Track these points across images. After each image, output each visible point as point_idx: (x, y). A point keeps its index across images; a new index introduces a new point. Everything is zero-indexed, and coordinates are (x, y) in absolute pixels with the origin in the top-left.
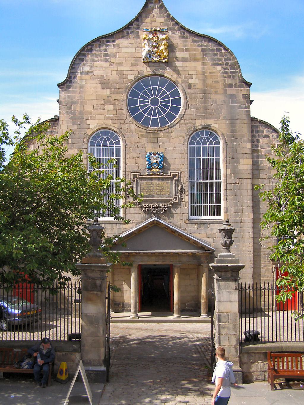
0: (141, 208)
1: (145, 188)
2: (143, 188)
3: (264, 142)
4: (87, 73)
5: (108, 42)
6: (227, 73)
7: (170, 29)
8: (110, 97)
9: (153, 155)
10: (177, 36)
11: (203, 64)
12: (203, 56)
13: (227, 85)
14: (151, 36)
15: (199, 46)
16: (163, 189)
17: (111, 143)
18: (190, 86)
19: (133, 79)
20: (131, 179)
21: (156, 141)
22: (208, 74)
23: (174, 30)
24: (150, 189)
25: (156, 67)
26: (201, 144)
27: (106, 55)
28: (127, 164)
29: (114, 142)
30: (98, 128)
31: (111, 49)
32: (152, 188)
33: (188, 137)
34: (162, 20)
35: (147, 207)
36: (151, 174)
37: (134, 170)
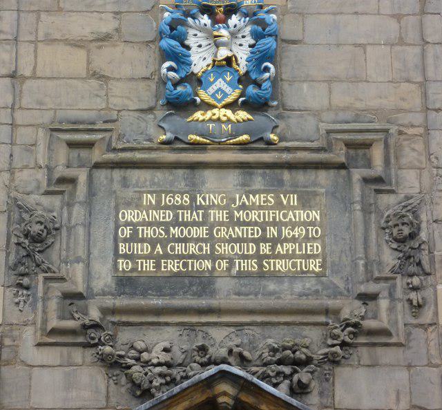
0: (113, 364)
1: (149, 232)
2: (135, 232)
9: (205, 20)
16: (274, 242)
20: (50, 169)
24: (185, 240)
32: (202, 232)
35: (164, 357)
37: (74, 114)
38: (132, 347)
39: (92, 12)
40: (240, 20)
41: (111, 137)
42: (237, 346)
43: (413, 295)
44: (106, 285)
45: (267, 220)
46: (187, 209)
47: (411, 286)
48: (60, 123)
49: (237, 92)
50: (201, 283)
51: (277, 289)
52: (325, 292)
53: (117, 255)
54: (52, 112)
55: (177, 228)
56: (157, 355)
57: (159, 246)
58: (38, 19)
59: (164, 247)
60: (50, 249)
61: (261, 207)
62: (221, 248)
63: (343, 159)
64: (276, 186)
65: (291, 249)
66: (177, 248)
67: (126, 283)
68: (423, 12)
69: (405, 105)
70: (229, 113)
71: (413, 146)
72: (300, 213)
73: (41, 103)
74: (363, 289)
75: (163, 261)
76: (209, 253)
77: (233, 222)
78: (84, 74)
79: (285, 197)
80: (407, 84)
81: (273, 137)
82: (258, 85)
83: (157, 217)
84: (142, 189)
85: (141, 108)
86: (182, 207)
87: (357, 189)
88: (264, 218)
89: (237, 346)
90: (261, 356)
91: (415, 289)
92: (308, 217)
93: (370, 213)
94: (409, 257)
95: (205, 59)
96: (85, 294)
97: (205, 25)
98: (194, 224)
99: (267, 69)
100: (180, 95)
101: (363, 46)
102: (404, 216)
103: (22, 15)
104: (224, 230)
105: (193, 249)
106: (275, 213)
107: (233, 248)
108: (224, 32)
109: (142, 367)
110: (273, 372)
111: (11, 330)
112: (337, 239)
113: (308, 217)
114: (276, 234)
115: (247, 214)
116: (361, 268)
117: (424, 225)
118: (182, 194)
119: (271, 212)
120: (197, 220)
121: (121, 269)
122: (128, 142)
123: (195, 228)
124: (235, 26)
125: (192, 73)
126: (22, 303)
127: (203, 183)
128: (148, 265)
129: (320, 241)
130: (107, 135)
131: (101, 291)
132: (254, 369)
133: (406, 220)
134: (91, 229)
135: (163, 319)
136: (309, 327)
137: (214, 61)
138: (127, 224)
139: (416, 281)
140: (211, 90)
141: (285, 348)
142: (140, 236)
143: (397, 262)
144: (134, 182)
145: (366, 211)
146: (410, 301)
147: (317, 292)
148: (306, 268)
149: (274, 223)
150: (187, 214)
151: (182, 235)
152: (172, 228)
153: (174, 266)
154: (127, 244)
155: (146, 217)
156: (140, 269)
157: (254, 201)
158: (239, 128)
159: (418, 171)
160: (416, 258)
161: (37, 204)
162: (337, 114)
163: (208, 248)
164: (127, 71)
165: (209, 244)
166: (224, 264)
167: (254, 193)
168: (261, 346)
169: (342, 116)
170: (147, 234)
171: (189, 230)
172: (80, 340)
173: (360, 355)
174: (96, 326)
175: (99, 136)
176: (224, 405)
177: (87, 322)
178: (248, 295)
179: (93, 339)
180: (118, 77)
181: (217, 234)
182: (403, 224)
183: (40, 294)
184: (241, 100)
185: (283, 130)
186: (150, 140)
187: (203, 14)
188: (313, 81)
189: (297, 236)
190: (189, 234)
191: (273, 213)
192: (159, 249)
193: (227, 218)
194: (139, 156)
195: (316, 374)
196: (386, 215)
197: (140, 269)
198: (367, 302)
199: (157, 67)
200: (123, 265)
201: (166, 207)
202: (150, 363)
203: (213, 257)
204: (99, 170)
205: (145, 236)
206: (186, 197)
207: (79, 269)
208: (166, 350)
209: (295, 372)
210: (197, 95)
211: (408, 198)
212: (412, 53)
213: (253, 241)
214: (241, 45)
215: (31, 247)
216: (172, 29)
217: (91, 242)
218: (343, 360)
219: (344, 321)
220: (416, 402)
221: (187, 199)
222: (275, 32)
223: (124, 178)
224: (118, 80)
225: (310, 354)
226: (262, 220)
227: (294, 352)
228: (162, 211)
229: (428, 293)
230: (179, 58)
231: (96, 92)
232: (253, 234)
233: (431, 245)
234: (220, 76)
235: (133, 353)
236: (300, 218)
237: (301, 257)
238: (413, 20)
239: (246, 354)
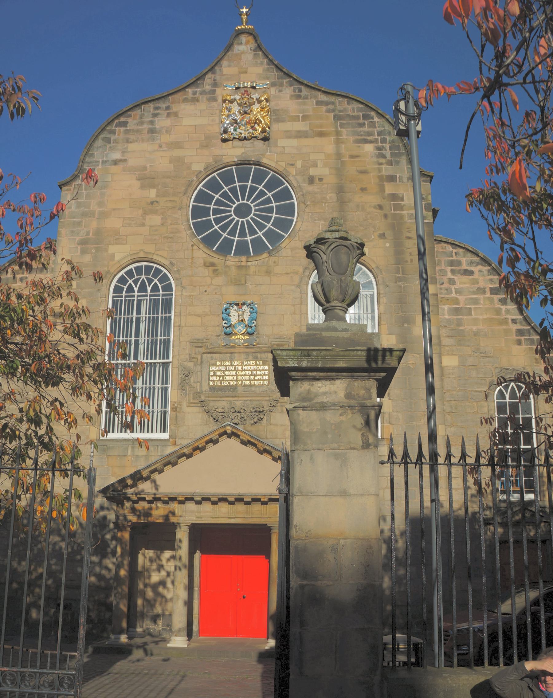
1: (218, 373)
2: (215, 373)
3: (465, 283)
4: (116, 162)
5: (157, 108)
6: (384, 156)
7: (273, 84)
8: (157, 202)
9: (236, 307)
10: (288, 96)
11: (338, 142)
12: (337, 128)
13: (385, 177)
14: (238, 97)
15: (328, 111)
16: (255, 376)
17: (155, 288)
18: (311, 180)
19: (202, 170)
21: (243, 282)
22: (346, 159)
23: (281, 85)
24: (229, 375)
25: (246, 147)
27: (152, 131)
29: (160, 286)
30: (129, 258)
31: (162, 122)
32: (234, 373)
33: (307, 273)
34: (259, 70)
53: (209, 380)
56: (220, 410)
59: (223, 378)
64: (256, 359)
67: (213, 389)
68: (301, 304)
70: (243, 337)
77: (243, 370)
82: (251, 327)
86: (228, 365)
98: (232, 370)
101: (283, 315)
135: (223, 399)
138: (212, 371)
140: (237, 330)
149: (255, 370)
158: (245, 341)
166: (240, 383)
172: (199, 405)
192: (221, 378)
194: (216, 350)
200: (211, 383)
201: (224, 366)
213: (249, 375)
221: (229, 363)
230: (228, 320)
239: (246, 409)
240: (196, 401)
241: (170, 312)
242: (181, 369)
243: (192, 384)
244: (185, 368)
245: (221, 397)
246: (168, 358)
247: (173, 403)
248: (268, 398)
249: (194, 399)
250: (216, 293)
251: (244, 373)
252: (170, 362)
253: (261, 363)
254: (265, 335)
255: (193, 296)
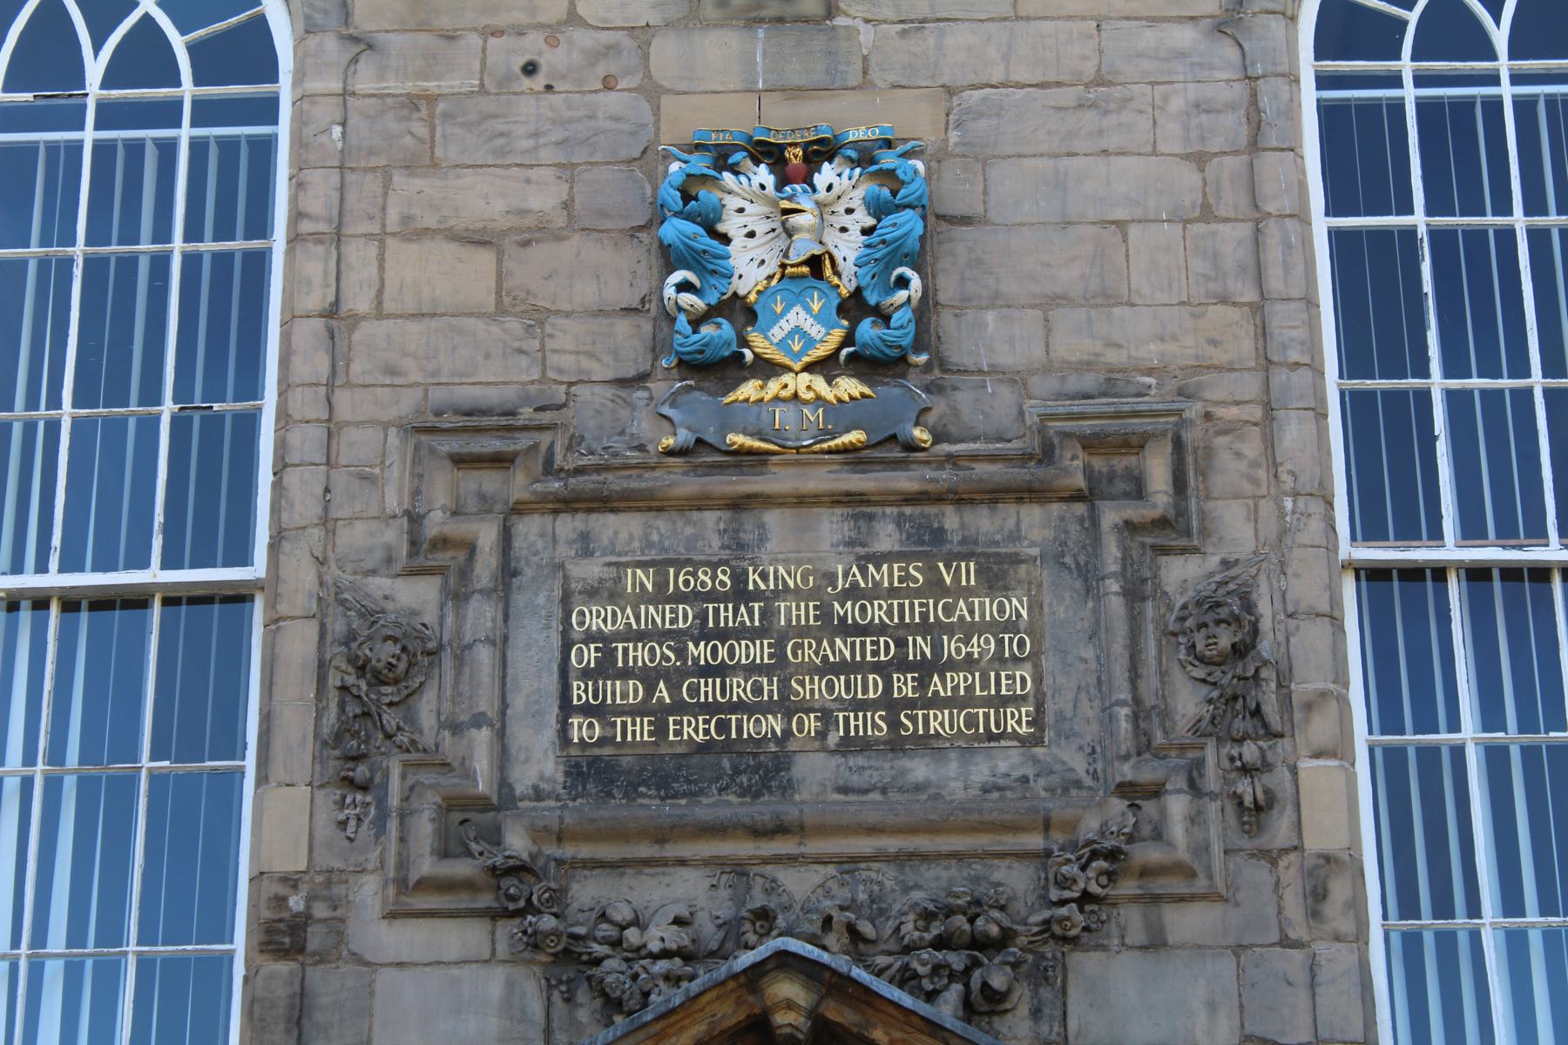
1: (640, 655)
2: (608, 655)
9: (763, 175)
16: (926, 669)
20: (415, 519)
24: (721, 671)
26: (1500, 37)
28: (355, 320)
29: (178, 43)
32: (760, 651)
35: (675, 938)
36: (738, 439)
37: (467, 394)
38: (603, 917)
39: (509, 166)
40: (839, 175)
41: (552, 444)
42: (842, 908)
43: (1244, 787)
44: (542, 777)
45: (907, 620)
46: (726, 603)
47: (1238, 764)
48: (438, 414)
49: (837, 335)
50: (759, 765)
51: (933, 777)
52: (1042, 782)
54: (419, 392)
55: (702, 643)
56: (659, 935)
57: (662, 685)
58: (387, 186)
59: (674, 688)
60: (416, 697)
61: (893, 592)
62: (804, 687)
63: (1079, 481)
65: (962, 685)
66: (703, 689)
69: (1219, 356)
70: (820, 384)
71: (1238, 446)
72: (982, 604)
73: (392, 371)
74: (1126, 772)
75: (671, 719)
76: (776, 698)
78: (490, 304)
79: (948, 567)
80: (1220, 308)
81: (920, 434)
82: (883, 316)
83: (659, 621)
84: (623, 559)
85: (620, 376)
86: (712, 596)
87: (1112, 551)
88: (902, 617)
89: (842, 908)
90: (898, 929)
91: (1246, 770)
92: (1001, 610)
93: (1144, 599)
94: (1235, 698)
95: (763, 262)
96: (495, 800)
97: (763, 187)
98: (741, 633)
99: (903, 282)
100: (706, 345)
101: (1121, 225)
102: (1218, 605)
103: (350, 177)
104: (810, 648)
105: (740, 691)
106: (927, 605)
107: (830, 687)
108: (805, 203)
109: (627, 960)
110: (924, 964)
111: (329, 883)
112: (1069, 661)
113: (1001, 610)
114: (928, 652)
115: (863, 609)
116: (1124, 726)
117: (1266, 624)
118: (714, 566)
119: (916, 602)
120: (748, 624)
121: (576, 740)
122: (592, 453)
123: (743, 643)
124: (830, 188)
125: (735, 294)
126: (353, 823)
127: (762, 540)
128: (638, 728)
129: (1028, 665)
130: (545, 438)
131: (531, 792)
132: (882, 960)
133: (1223, 612)
134: (509, 653)
135: (673, 850)
136: (1007, 862)
137: (783, 266)
138: (589, 638)
139: (1250, 752)
140: (777, 333)
141: (950, 911)
142: (620, 664)
143: (1206, 711)
144: (606, 542)
145: (1134, 594)
146: (1238, 800)
147: (1025, 780)
148: (998, 726)
149: (925, 628)
150: (726, 610)
151: (715, 659)
152: (691, 645)
153: (696, 730)
154: (590, 683)
155: (632, 620)
156: (619, 739)
157: (878, 577)
158: (840, 414)
159: (1251, 503)
160: (1248, 700)
161: (386, 598)
162: (1063, 379)
163: (775, 688)
164: (586, 293)
165: (775, 679)
166: (811, 723)
167: (879, 559)
168: (897, 907)
169: (1073, 383)
170: (635, 658)
171: (731, 648)
172: (486, 900)
173: (1122, 923)
174: (519, 869)
175: (523, 441)
176: (788, 1030)
177: (499, 860)
178: (865, 792)
179: (513, 899)
180: (566, 307)
181: (795, 655)
182: (1218, 622)
183: (394, 801)
184: (845, 352)
185: (941, 418)
186: (641, 448)
187: (757, 162)
188: (1009, 307)
189: (976, 656)
190: (731, 654)
191: (921, 605)
193: (816, 618)
194: (615, 482)
195: (1024, 968)
196: (1178, 604)
197: (619, 739)
198: (1137, 802)
199: (654, 283)
200: (579, 728)
201: (679, 598)
202: (643, 952)
203: (787, 707)
204: (526, 519)
205: (631, 664)
206: (724, 572)
207: (482, 738)
208: (678, 921)
209: (976, 963)
210: (744, 343)
211: (1226, 564)
212: (1232, 238)
213: (877, 668)
214: (844, 230)
215: (373, 696)
216: (687, 197)
217: (509, 679)
218: (1086, 934)
219: (1083, 847)
220: (1249, 1029)
222: (920, 198)
223: (585, 537)
224: (568, 315)
225: (1006, 923)
226: (896, 620)
227: (972, 921)
228: (667, 607)
229: (1279, 779)
231: (516, 344)
232: (875, 653)
233: (1284, 666)
234: (799, 299)
235: (605, 930)
236: (983, 615)
237: (987, 702)
238: (1233, 163)
239: (866, 928)
240: (461, 868)
241: (260, 225)
242: (338, 627)
243: (428, 740)
244: (370, 615)
245: (661, 841)
246: (244, 559)
247: (271, 888)
248: (1035, 841)
249: (444, 853)
250: (608, 84)
251: (842, 648)
252: (257, 585)
253: (968, 573)
254: (994, 370)
255: (432, 99)
